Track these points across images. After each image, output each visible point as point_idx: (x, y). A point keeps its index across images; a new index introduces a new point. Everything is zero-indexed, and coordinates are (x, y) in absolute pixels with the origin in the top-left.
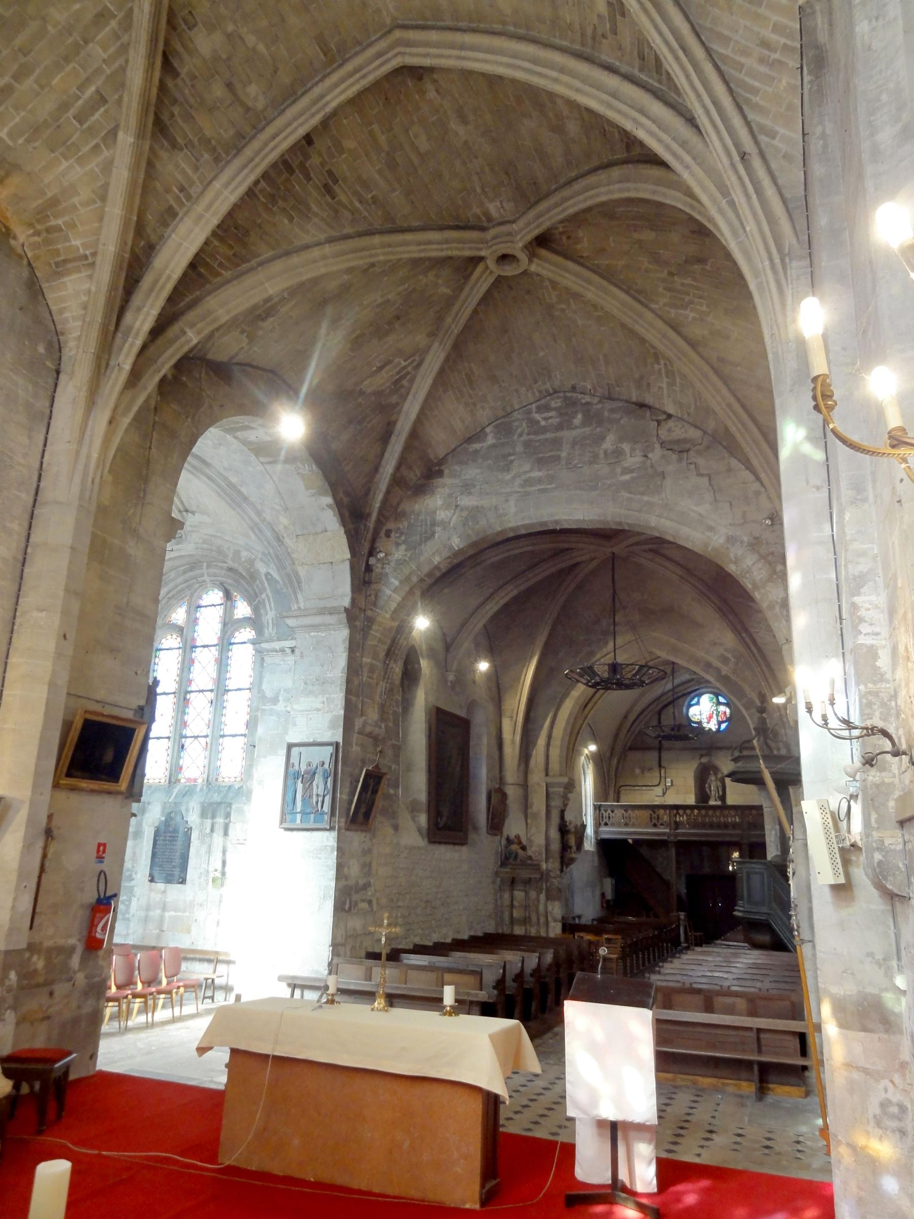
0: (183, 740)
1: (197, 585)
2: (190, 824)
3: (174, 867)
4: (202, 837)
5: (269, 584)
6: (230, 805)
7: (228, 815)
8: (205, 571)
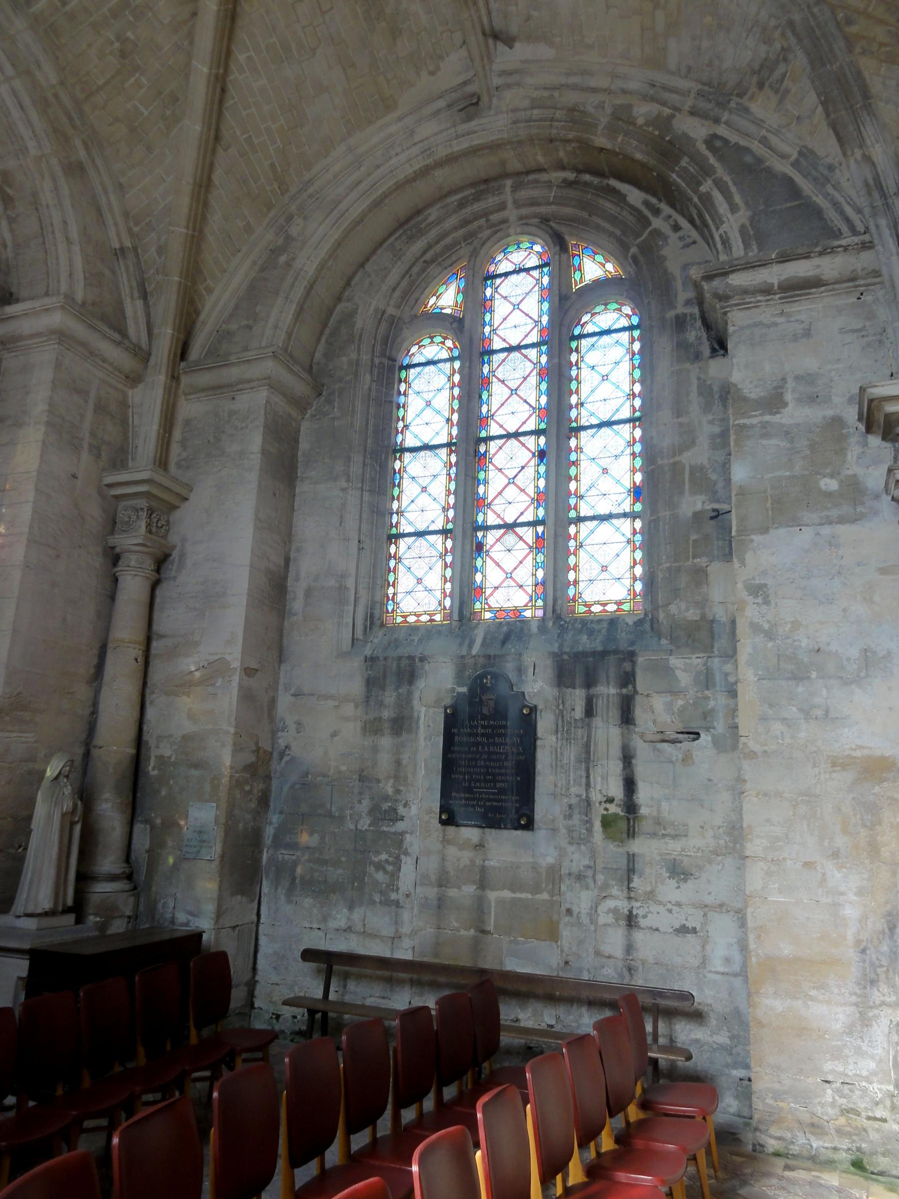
0: (480, 534)
1: (488, 232)
2: (532, 701)
3: (502, 791)
4: (563, 727)
5: (720, 159)
6: (631, 656)
7: (627, 679)
8: (508, 196)
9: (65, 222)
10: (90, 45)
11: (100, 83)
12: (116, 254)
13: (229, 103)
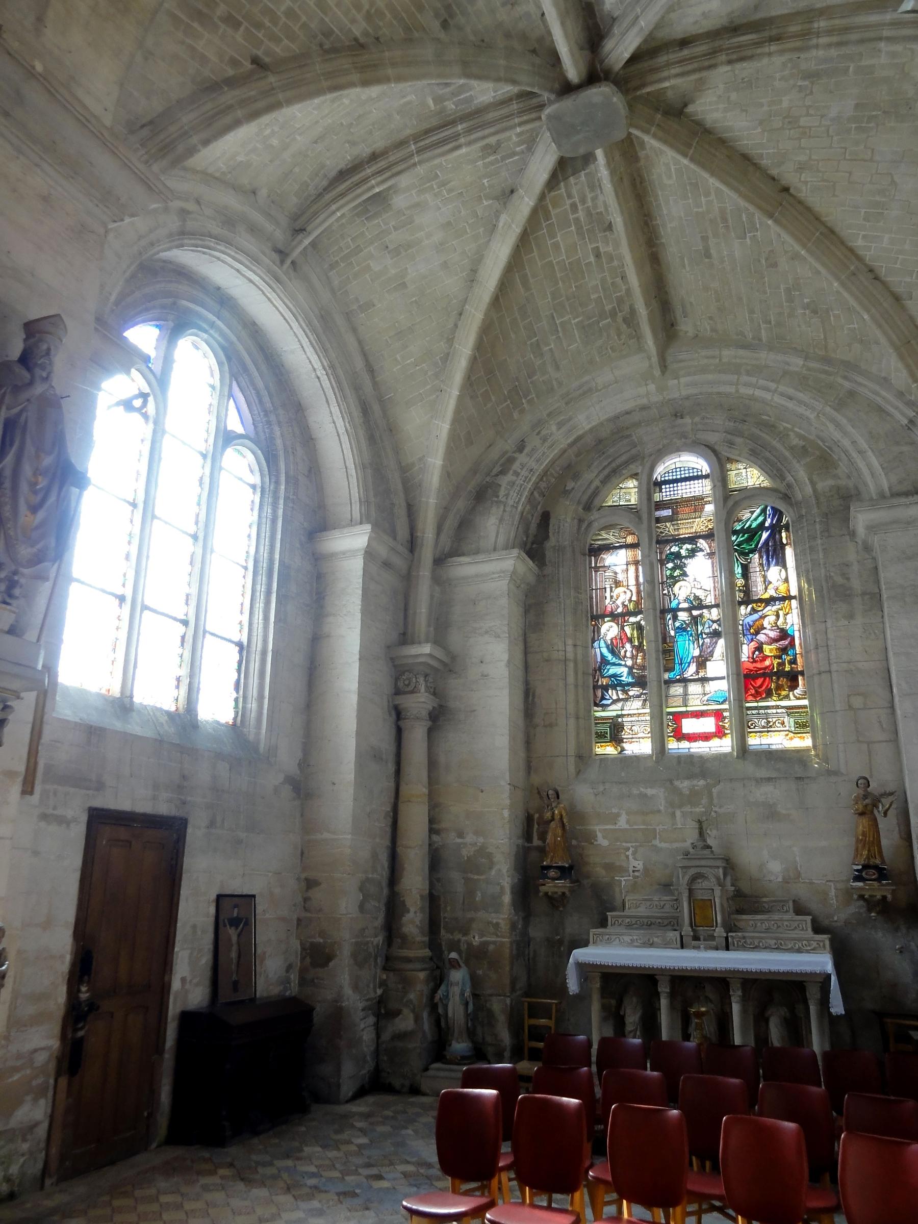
9: (854, 442)
10: (799, 326)
11: (822, 337)
12: (909, 428)
13: (882, 273)
